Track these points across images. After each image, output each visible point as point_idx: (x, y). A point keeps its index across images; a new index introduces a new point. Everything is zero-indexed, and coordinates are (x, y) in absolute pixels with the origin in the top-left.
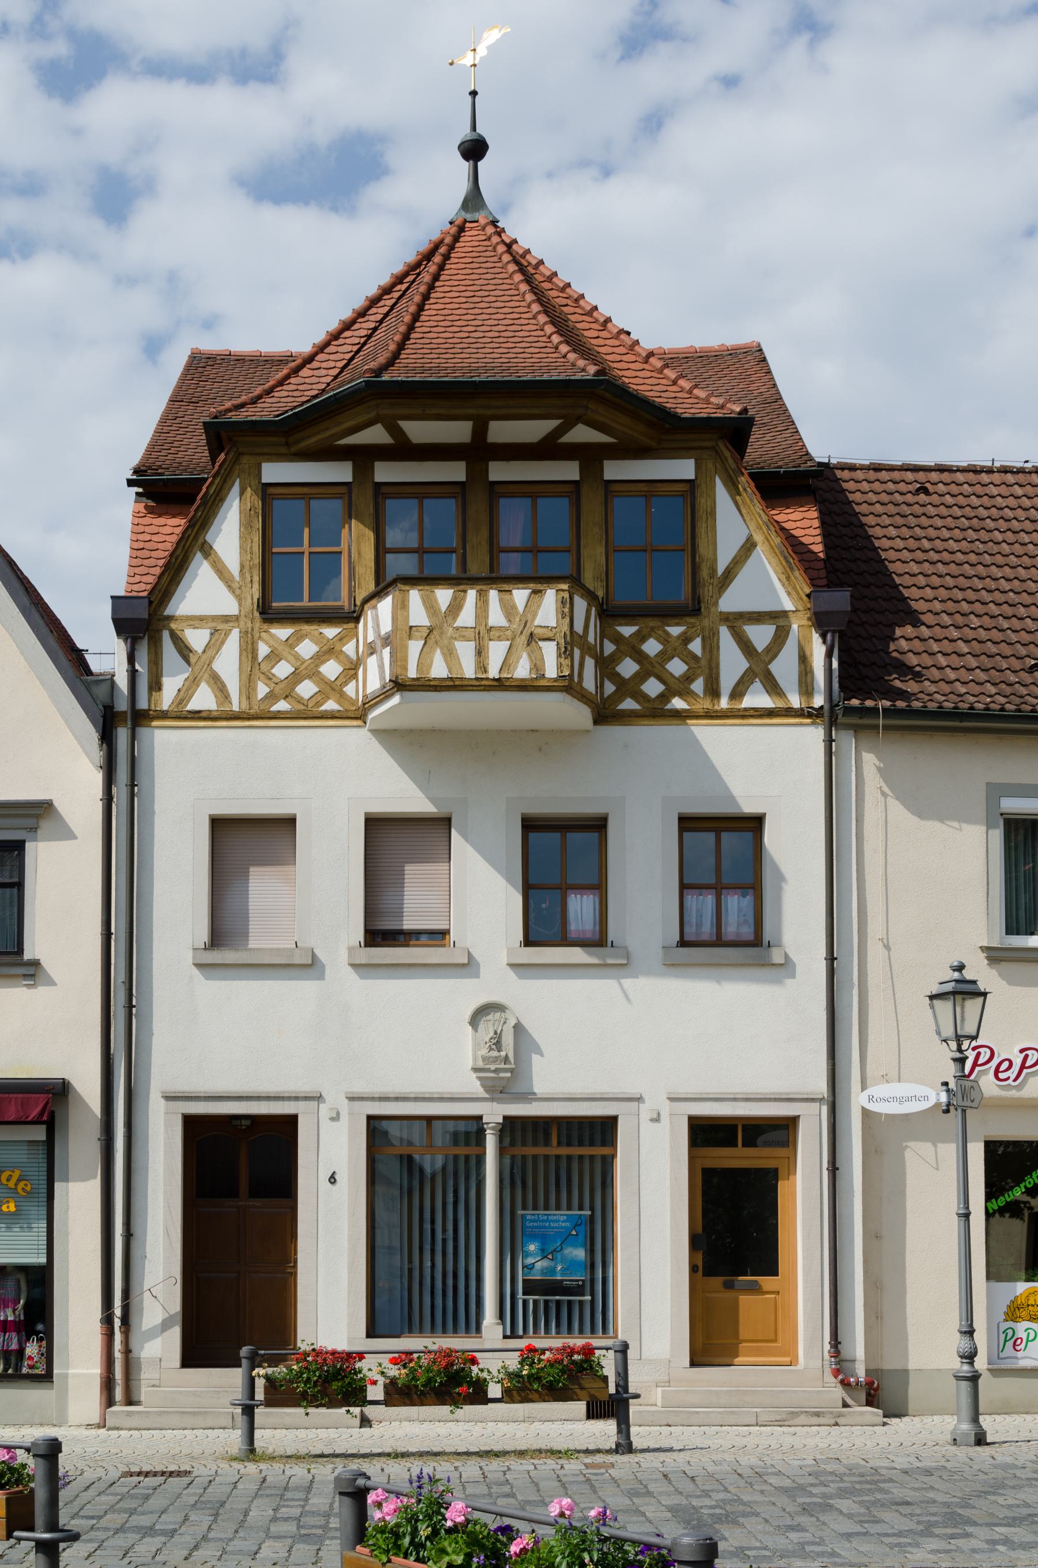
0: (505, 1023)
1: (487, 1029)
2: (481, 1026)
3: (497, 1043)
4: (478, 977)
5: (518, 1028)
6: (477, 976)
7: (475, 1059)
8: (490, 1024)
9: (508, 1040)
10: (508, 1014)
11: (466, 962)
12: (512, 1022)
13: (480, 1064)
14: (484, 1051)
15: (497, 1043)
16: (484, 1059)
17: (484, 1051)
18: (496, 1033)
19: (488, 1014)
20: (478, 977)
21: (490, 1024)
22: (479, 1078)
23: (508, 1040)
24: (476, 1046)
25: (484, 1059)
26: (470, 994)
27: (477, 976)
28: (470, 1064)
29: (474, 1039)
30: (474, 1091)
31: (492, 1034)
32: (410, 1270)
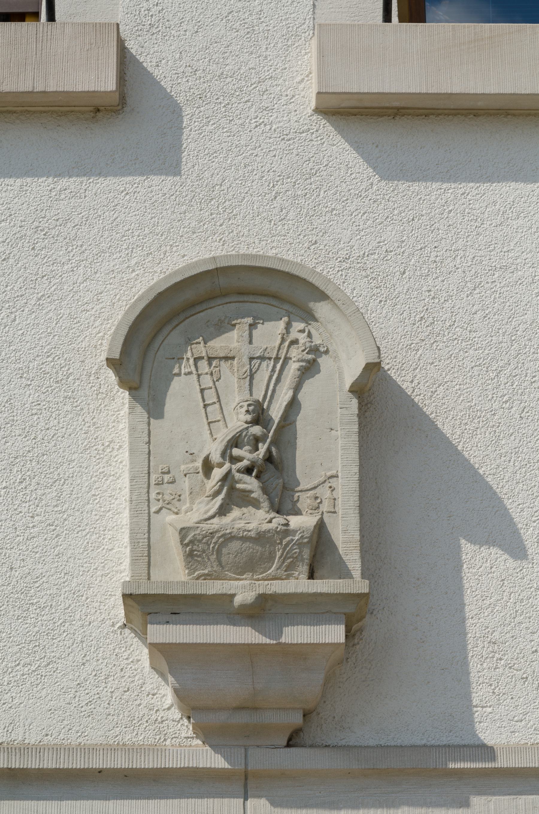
0: (309, 369)
1: (208, 407)
2: (182, 391)
3: (267, 461)
4: (174, 169)
5: (373, 390)
6: (167, 161)
7: (145, 554)
8: (231, 379)
9: (328, 454)
10: (329, 326)
11: (109, 83)
12: (346, 365)
13: (174, 574)
14: (198, 510)
15: (267, 461)
16: (197, 548)
17: (198, 510)
18: (259, 416)
19: (222, 327)
20: (174, 169)
21: (231, 379)
22: (168, 657)
23: (328, 454)
24: (153, 484)
25: (197, 548)
26: (131, 236)
27: (167, 161)
28: (119, 570)
29: (145, 451)
30: (144, 736)
31: (237, 420)
32: (60, 809)
